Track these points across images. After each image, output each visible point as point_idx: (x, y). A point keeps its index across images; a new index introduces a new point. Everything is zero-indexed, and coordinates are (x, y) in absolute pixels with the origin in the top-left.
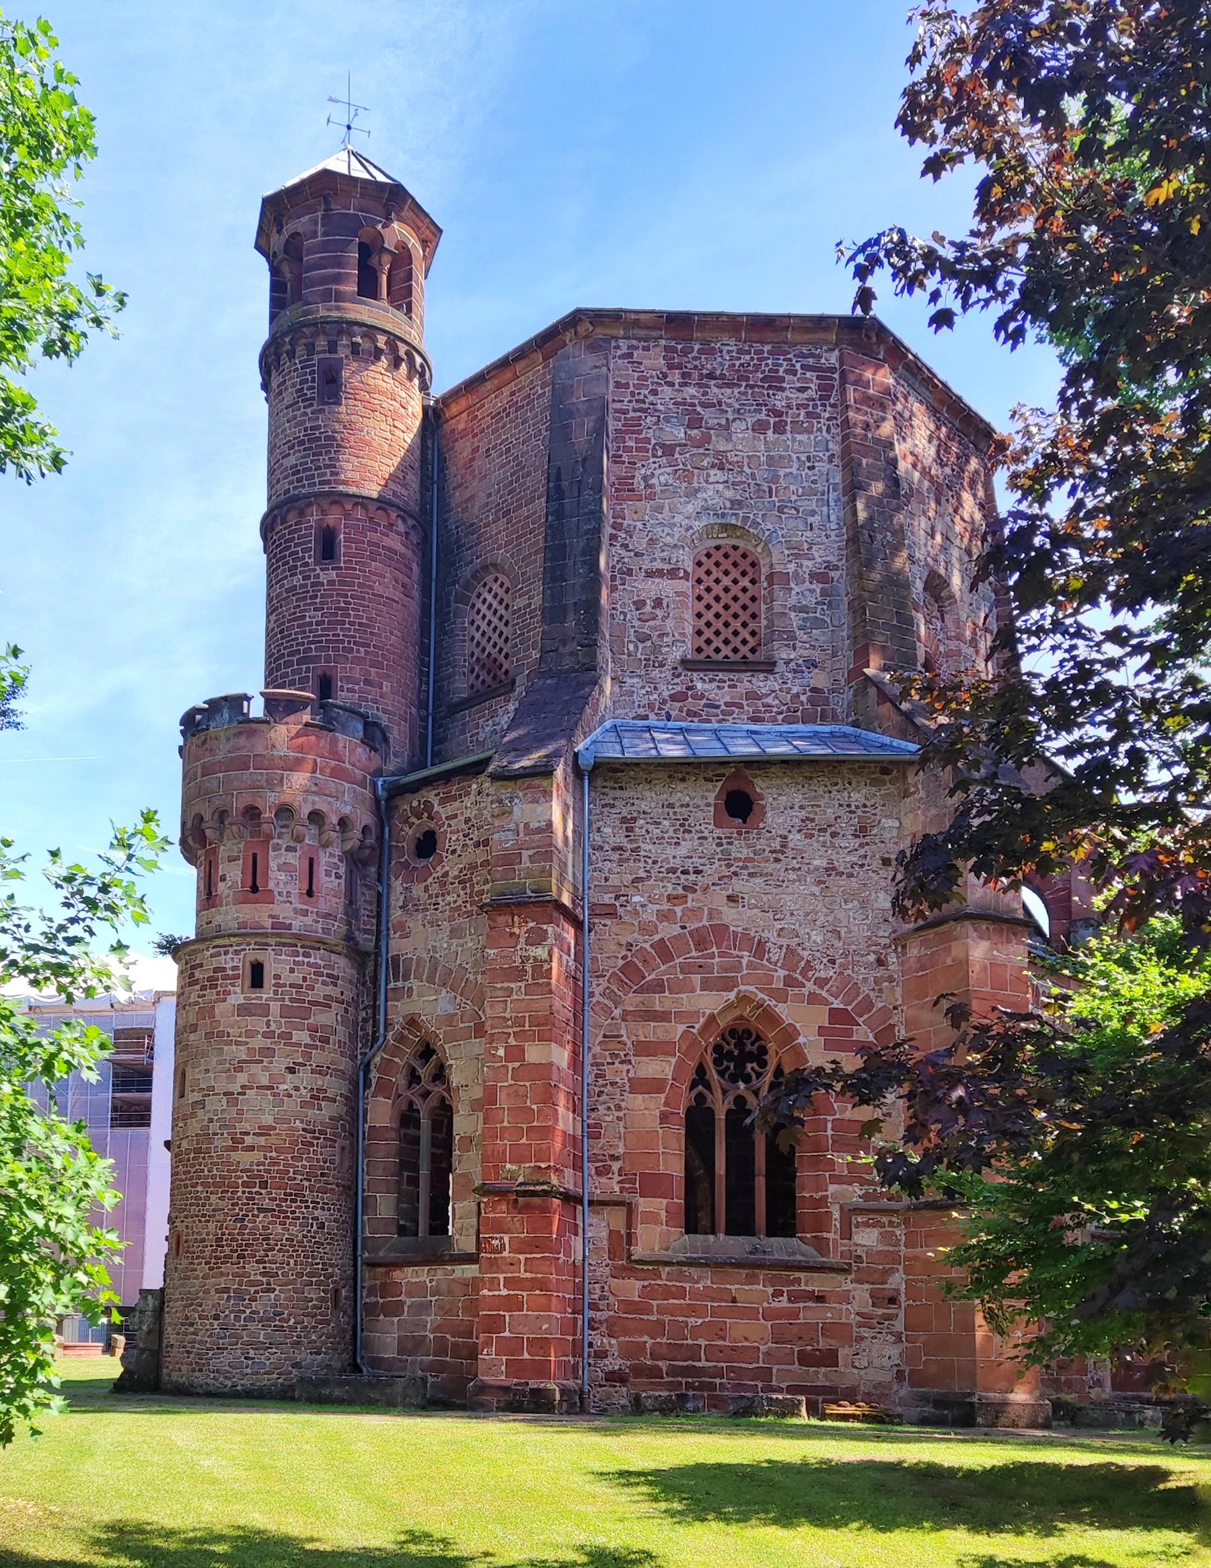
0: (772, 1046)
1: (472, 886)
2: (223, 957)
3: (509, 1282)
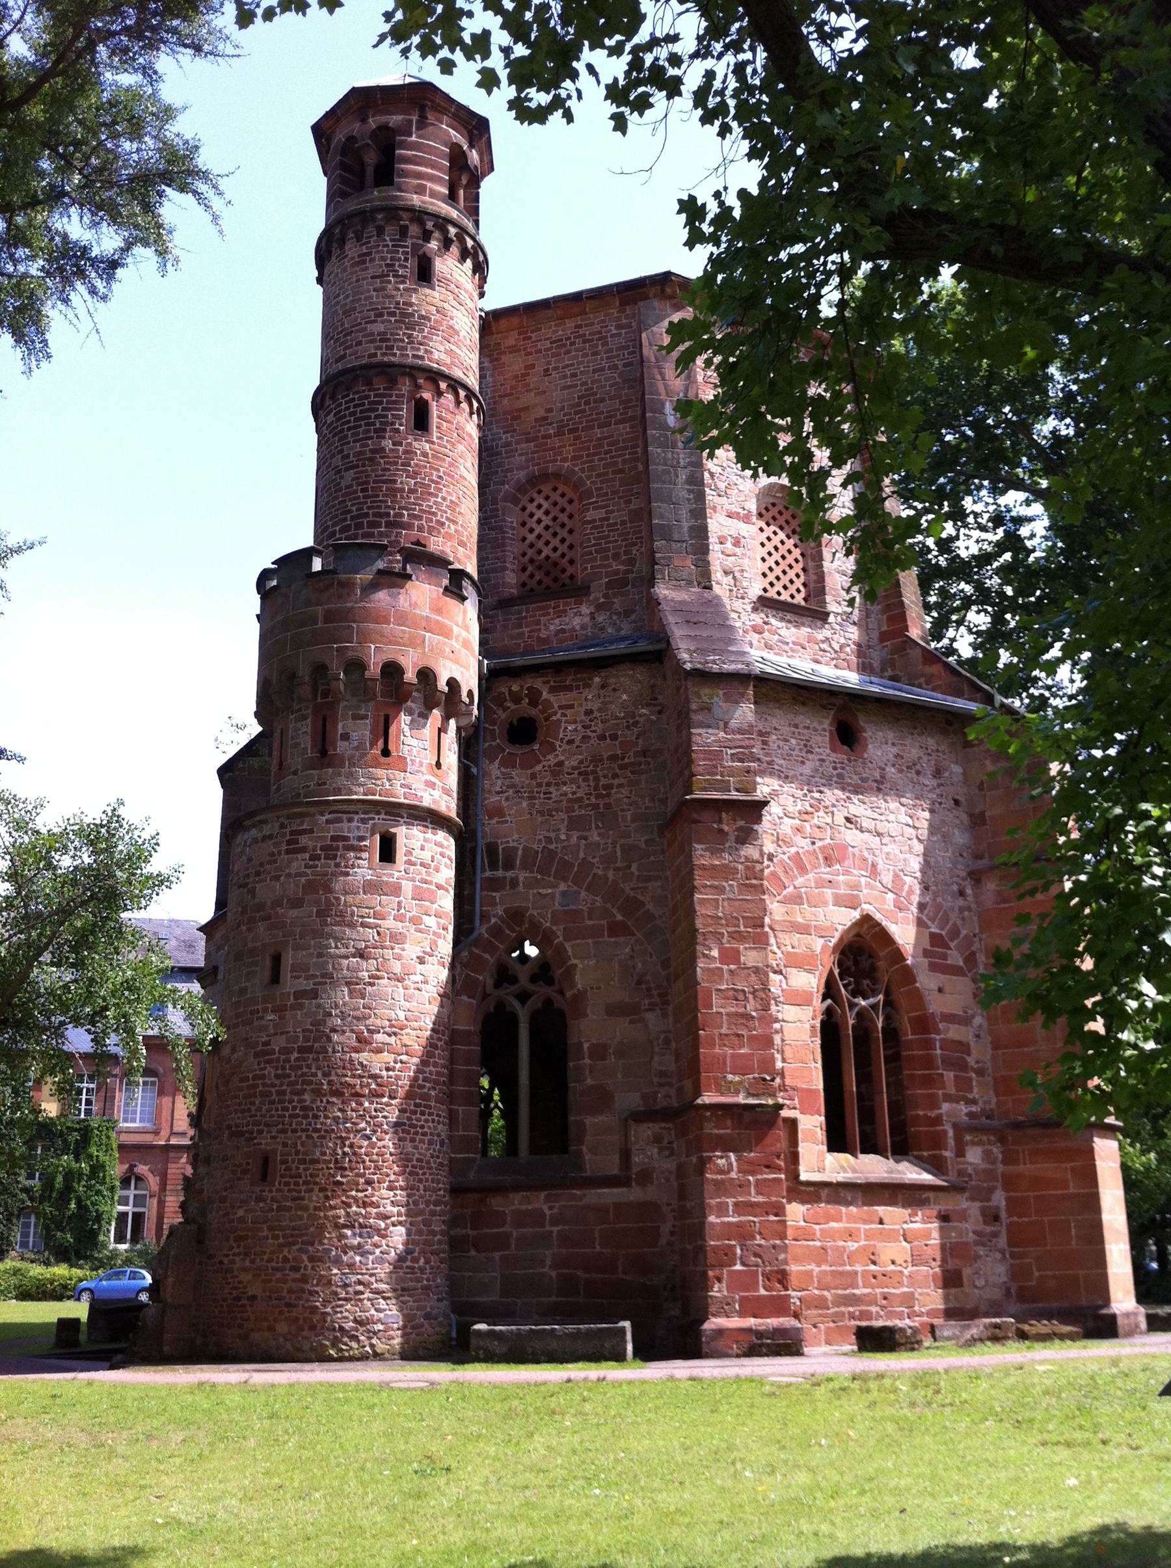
0: (881, 964)
1: (597, 779)
2: (345, 825)
3: (740, 1208)
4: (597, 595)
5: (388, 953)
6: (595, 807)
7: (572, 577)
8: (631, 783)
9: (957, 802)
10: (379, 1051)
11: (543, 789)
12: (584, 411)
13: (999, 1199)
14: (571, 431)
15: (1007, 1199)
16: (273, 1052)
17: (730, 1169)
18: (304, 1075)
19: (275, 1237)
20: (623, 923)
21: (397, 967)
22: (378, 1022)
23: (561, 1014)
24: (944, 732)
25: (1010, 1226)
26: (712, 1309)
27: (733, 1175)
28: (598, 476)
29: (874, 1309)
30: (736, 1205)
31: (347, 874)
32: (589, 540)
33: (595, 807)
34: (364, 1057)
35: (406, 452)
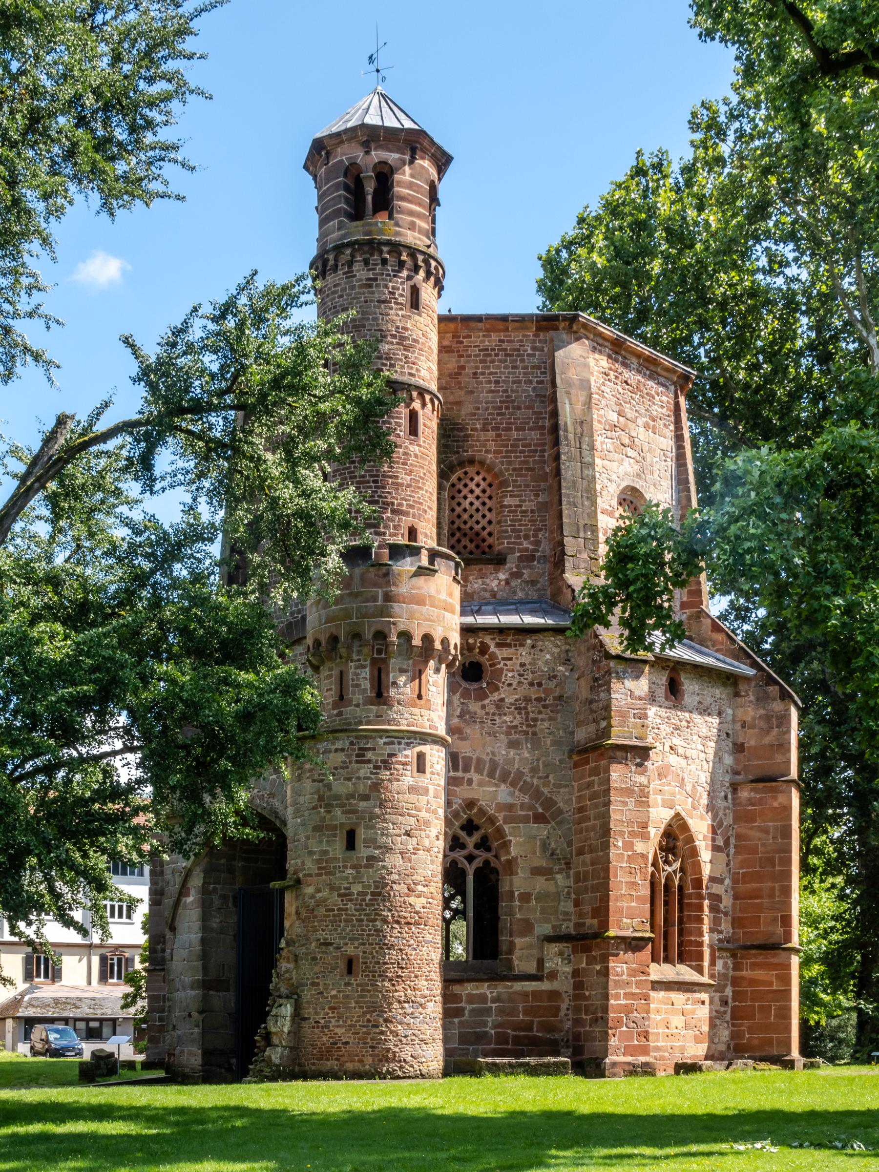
0: (679, 844)
1: (527, 713)
2: (396, 746)
3: (627, 996)
4: (511, 564)
5: (423, 833)
6: (526, 733)
7: (490, 547)
8: (550, 719)
9: (728, 734)
10: (419, 896)
11: (490, 717)
12: (504, 414)
13: (729, 991)
14: (494, 429)
15: (733, 992)
16: (352, 894)
17: (623, 974)
18: (375, 910)
19: (362, 1008)
20: (543, 815)
21: (427, 843)
22: (419, 878)
23: (495, 871)
24: (724, 685)
25: (733, 1008)
26: (610, 1051)
27: (624, 977)
28: (514, 470)
29: (666, 1054)
30: (625, 994)
31: (398, 780)
32: (506, 521)
33: (526, 733)
34: (412, 900)
35: (405, 454)
